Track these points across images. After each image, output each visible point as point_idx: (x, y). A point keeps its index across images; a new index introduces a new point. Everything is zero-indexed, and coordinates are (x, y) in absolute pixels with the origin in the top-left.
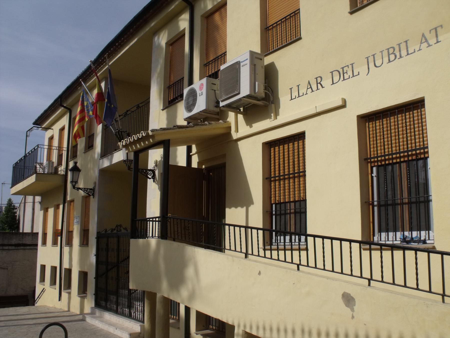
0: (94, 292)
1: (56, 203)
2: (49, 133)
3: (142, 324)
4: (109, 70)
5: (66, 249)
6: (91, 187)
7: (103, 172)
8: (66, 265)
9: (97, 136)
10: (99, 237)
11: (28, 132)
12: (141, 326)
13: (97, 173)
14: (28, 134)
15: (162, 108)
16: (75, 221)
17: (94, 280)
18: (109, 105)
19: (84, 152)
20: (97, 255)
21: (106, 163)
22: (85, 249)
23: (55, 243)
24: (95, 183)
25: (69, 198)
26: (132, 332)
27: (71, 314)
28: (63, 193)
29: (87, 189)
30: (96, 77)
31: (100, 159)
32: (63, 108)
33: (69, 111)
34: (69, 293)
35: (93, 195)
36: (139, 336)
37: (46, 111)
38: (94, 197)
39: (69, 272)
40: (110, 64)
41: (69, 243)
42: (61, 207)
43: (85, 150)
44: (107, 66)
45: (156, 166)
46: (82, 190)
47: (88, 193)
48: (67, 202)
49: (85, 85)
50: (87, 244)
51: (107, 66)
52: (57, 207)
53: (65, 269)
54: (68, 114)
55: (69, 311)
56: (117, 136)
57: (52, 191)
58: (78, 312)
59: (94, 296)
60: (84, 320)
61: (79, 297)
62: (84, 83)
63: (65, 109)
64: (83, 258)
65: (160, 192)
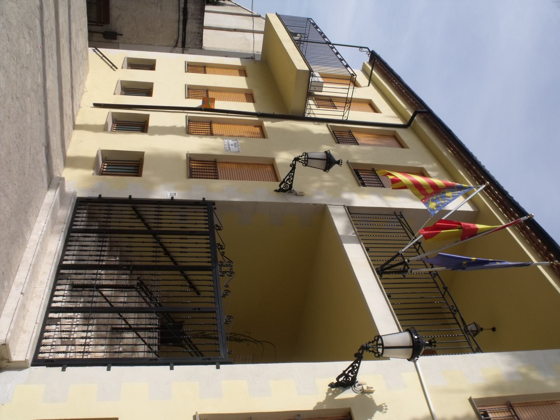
0: (106, 195)
1: (256, 94)
2: (361, 79)
3: (30, 362)
4: (527, 264)
5: (180, 120)
6: (294, 187)
7: (322, 213)
8: (156, 119)
9: (380, 195)
10: (207, 206)
11: (367, 50)
12: (26, 361)
13: (319, 199)
14: (364, 49)
15: (475, 396)
16: (231, 142)
17: (127, 196)
18: (465, 263)
19: (350, 161)
20: (172, 202)
21: (341, 224)
22: (183, 169)
23: (191, 91)
24: (301, 195)
25: (267, 124)
26: (10, 346)
27: (66, 132)
28: (277, 113)
29: (292, 181)
30: (504, 224)
31: (344, 206)
32: (411, 115)
33: (406, 124)
34: (104, 129)
35: (280, 190)
36: (3, 359)
37: (398, 78)
38: (276, 191)
39: (141, 126)
40: (540, 267)
41: (191, 128)
42: (250, 107)
43: (351, 163)
44: (535, 262)
45: (363, 392)
46: (291, 172)
47: (284, 182)
48: (261, 119)
49: (481, 192)
50: (192, 174)
51: (535, 262)
52: (250, 97)
53: (148, 115)
54: (399, 122)
55: (75, 127)
56: (393, 258)
57: (276, 87)
58: (70, 153)
59: (96, 195)
60: (50, 186)
61: (97, 156)
62: (484, 189)
63: (408, 119)
64: (165, 160)
65: (311, 408)
